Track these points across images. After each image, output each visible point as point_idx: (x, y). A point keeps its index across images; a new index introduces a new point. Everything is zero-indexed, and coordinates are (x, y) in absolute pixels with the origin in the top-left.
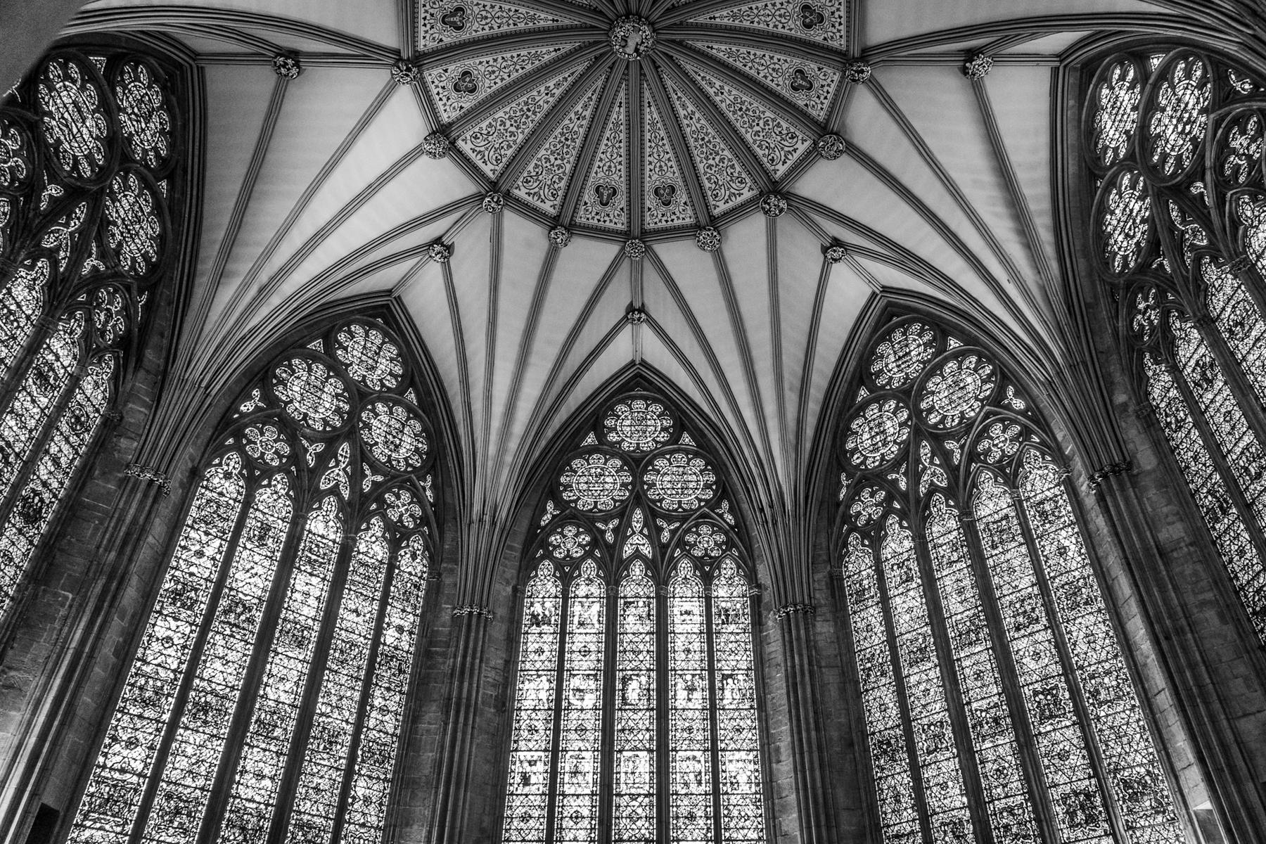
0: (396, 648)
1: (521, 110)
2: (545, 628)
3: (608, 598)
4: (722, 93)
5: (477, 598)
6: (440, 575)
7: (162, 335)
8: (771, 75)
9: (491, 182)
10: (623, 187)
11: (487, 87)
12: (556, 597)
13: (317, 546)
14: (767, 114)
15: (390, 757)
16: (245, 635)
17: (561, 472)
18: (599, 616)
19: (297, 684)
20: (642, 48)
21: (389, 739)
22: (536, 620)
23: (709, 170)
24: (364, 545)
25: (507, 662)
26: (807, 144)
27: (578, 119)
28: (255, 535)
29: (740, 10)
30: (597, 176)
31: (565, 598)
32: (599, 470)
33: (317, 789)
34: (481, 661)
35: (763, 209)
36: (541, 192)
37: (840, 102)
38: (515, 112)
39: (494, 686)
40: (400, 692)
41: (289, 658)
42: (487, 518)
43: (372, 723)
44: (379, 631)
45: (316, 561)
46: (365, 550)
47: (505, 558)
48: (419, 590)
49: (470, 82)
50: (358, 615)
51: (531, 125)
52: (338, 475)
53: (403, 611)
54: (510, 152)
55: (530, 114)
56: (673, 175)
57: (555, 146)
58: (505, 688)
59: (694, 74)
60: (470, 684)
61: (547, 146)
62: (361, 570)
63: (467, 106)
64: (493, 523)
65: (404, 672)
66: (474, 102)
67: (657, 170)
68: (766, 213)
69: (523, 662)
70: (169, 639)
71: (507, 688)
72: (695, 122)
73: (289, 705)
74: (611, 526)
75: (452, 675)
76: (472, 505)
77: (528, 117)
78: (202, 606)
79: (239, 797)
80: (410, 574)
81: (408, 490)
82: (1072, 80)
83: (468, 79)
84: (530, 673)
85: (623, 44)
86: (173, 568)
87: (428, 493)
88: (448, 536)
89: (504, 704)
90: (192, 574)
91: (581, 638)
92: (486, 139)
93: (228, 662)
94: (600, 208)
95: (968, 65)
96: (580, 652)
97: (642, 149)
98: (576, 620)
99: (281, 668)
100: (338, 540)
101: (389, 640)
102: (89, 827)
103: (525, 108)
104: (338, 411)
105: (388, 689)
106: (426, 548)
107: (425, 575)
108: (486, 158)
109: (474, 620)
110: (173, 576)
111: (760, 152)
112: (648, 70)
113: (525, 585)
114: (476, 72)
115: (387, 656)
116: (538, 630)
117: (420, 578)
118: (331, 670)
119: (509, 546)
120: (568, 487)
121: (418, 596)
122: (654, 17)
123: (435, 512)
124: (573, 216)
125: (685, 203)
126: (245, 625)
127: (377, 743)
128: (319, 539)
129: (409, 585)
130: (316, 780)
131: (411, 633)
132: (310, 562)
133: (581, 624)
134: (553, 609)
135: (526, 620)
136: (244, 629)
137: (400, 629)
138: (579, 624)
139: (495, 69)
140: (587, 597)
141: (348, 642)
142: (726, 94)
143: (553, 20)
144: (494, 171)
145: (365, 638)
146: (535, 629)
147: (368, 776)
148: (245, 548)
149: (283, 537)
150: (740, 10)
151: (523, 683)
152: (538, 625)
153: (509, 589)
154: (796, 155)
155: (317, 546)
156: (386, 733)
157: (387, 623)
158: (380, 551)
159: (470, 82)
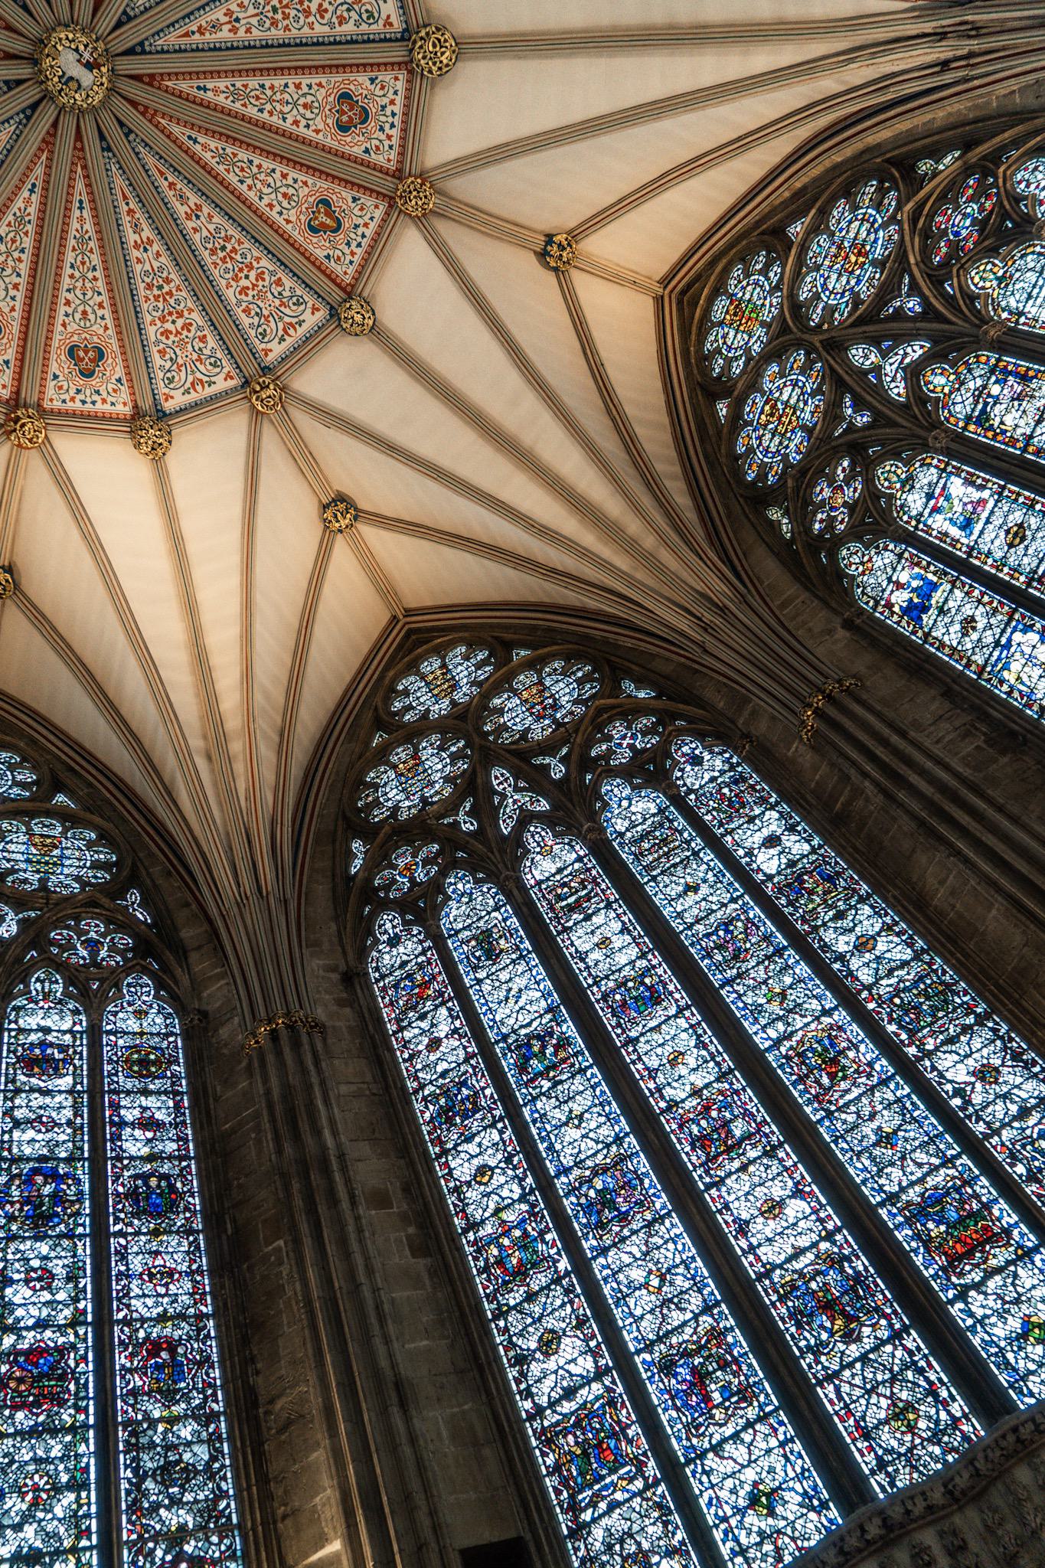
0: (791, 864)
1: (156, 298)
2: (937, 597)
3: (950, 454)
5: (804, 689)
6: (747, 736)
7: (188, 905)
9: (242, 387)
10: (323, 184)
11: (102, 330)
12: (900, 556)
13: (565, 885)
15: (948, 985)
16: (573, 1065)
17: (738, 474)
18: (972, 484)
19: (701, 1044)
21: (917, 968)
22: (914, 611)
24: (619, 821)
25: (948, 694)
27: (198, 217)
28: (479, 959)
31: (909, 538)
32: (767, 408)
33: (886, 1139)
34: (903, 734)
36: (287, 319)
38: (156, 308)
39: (966, 735)
40: (862, 900)
41: (657, 1029)
42: (708, 617)
43: (865, 976)
44: (742, 874)
45: (577, 901)
46: (626, 823)
47: (794, 618)
48: (744, 780)
49: (86, 352)
50: (695, 889)
51: (183, 294)
52: (515, 802)
53: (751, 820)
54: (212, 342)
55: (166, 289)
57: (227, 271)
58: (985, 717)
60: (922, 772)
61: (224, 282)
62: (646, 846)
63: (119, 372)
64: (722, 610)
65: (838, 874)
66: (119, 360)
67: (309, 115)
69: (968, 666)
70: (483, 1170)
71: (988, 715)
73: (718, 1080)
74: (849, 411)
75: (889, 797)
76: (682, 634)
77: (170, 293)
78: (488, 1092)
79: (775, 1267)
80: (713, 779)
81: (611, 720)
83: (81, 354)
84: (993, 659)
86: (416, 1092)
87: (642, 695)
88: (709, 694)
89: (1013, 734)
90: (443, 1075)
91: (988, 536)
92: (179, 367)
93: (580, 1117)
94: (340, 237)
96: (1011, 545)
98: (955, 532)
99: (659, 1051)
100: (582, 853)
101: (771, 867)
102: (594, 1520)
103: (156, 292)
104: (454, 758)
105: (840, 915)
106: (700, 736)
107: (734, 760)
108: (205, 379)
109: (832, 712)
110: (424, 1099)
113: (853, 603)
114: (76, 338)
115: (789, 885)
116: (933, 612)
117: (732, 768)
118: (729, 982)
119: (783, 606)
120: (762, 476)
121: (752, 787)
123: (670, 698)
126: (562, 1055)
127: (906, 990)
128: (558, 877)
129: (726, 791)
130: (868, 1129)
131: (791, 829)
132: (571, 909)
133: (967, 525)
134: (917, 570)
135: (905, 628)
136: (564, 1061)
137: (772, 841)
138: (963, 528)
139: (81, 308)
140: (930, 496)
141: (717, 930)
144: (229, 376)
145: (733, 900)
146: (927, 619)
147: (943, 1043)
148: (479, 982)
149: (514, 922)
151: (1002, 682)
152: (925, 609)
153: (841, 633)
155: (565, 885)
156: (904, 964)
157: (746, 855)
158: (646, 805)
159: (86, 352)
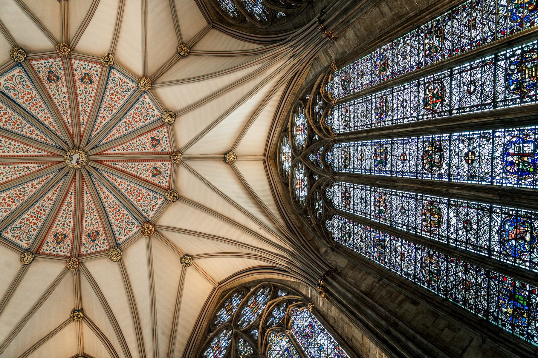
4: (122, 185)
8: (143, 172)
14: (143, 191)
20: (80, 161)
23: (116, 222)
26: (162, 200)
29: (126, 145)
30: (57, 228)
35: (142, 231)
37: (174, 175)
56: (98, 226)
59: (108, 177)
68: (144, 233)
72: (109, 200)
82: (271, 162)
85: (70, 159)
95: (225, 156)
97: (82, 214)
111: (141, 209)
112: (85, 175)
122: (89, 153)
124: (38, 249)
125: (104, 239)
142: (124, 185)
143: (38, 152)
150: (126, 145)
154: (157, 206)
